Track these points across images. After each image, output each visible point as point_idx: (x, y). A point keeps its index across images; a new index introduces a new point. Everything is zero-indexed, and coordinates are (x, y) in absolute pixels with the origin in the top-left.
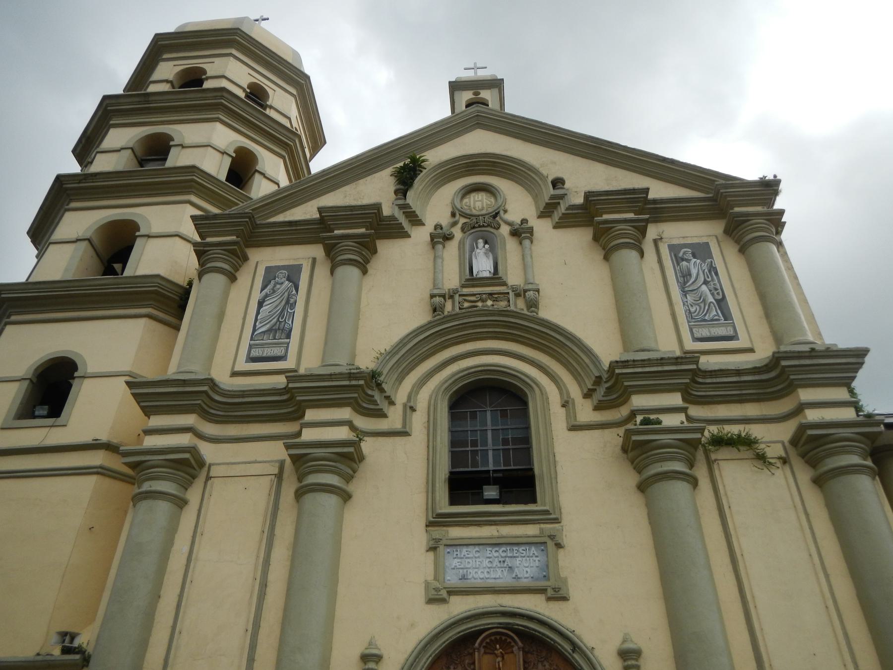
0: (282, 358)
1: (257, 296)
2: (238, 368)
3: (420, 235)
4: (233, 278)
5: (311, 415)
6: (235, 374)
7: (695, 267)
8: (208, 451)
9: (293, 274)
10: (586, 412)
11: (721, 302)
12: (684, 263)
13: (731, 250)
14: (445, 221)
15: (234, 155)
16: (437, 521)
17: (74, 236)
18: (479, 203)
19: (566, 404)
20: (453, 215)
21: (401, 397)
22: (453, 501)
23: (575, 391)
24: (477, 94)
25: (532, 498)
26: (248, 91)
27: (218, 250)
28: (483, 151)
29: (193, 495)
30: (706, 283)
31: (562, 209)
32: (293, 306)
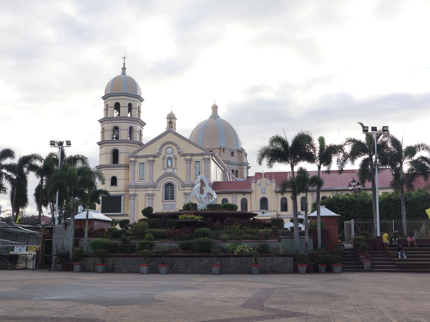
0: (144, 179)
1: (139, 168)
2: (138, 181)
3: (161, 157)
4: (135, 165)
5: (148, 189)
6: (138, 181)
7: (197, 165)
8: (137, 193)
9: (143, 163)
10: (181, 188)
11: (200, 172)
12: (196, 165)
13: (203, 161)
14: (165, 155)
15: (129, 130)
16: (163, 202)
17: (108, 152)
18: (169, 150)
19: (179, 187)
20: (166, 153)
21: (159, 185)
22: (166, 199)
23: (180, 185)
24: (171, 120)
25: (173, 199)
26: (129, 107)
27: (133, 161)
28: (170, 141)
29: (136, 198)
30: (198, 169)
31: (181, 153)
32: (144, 170)
